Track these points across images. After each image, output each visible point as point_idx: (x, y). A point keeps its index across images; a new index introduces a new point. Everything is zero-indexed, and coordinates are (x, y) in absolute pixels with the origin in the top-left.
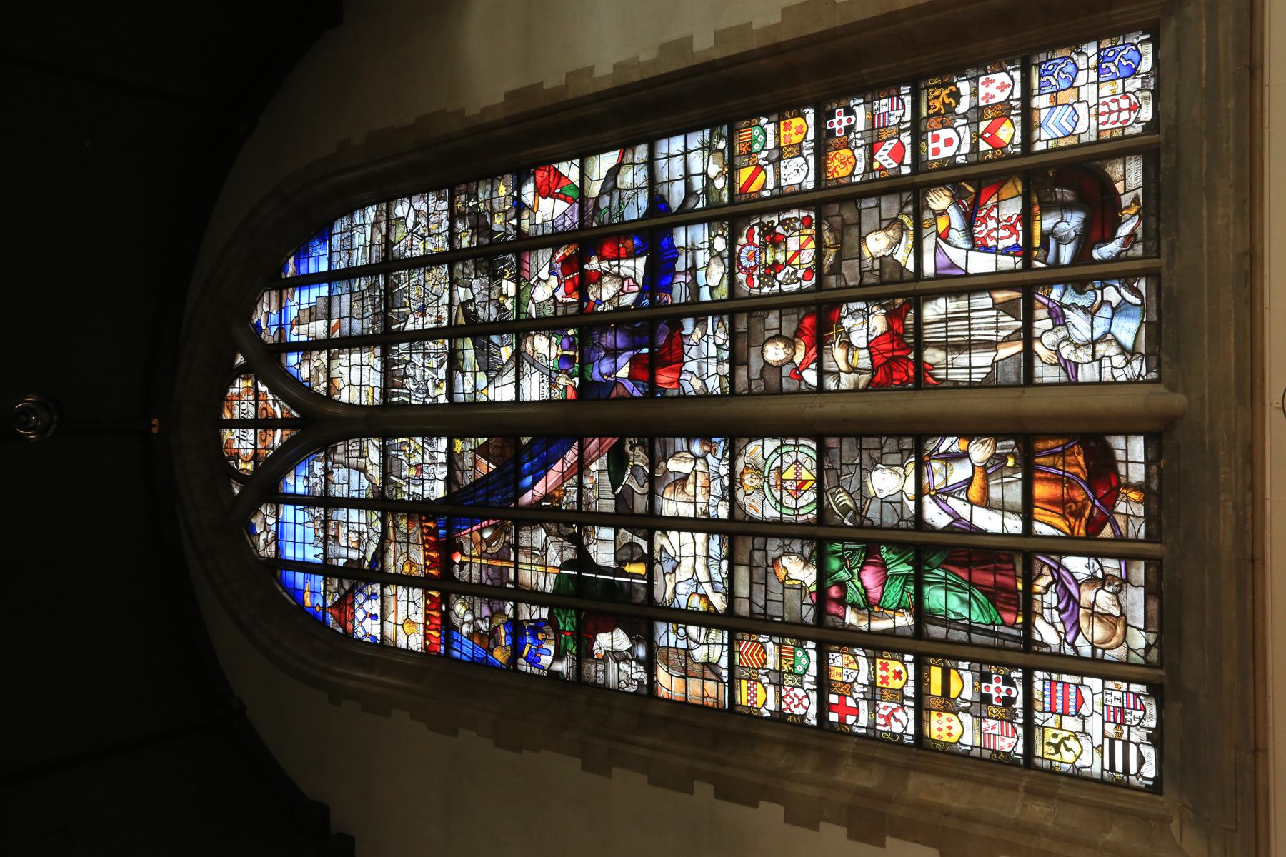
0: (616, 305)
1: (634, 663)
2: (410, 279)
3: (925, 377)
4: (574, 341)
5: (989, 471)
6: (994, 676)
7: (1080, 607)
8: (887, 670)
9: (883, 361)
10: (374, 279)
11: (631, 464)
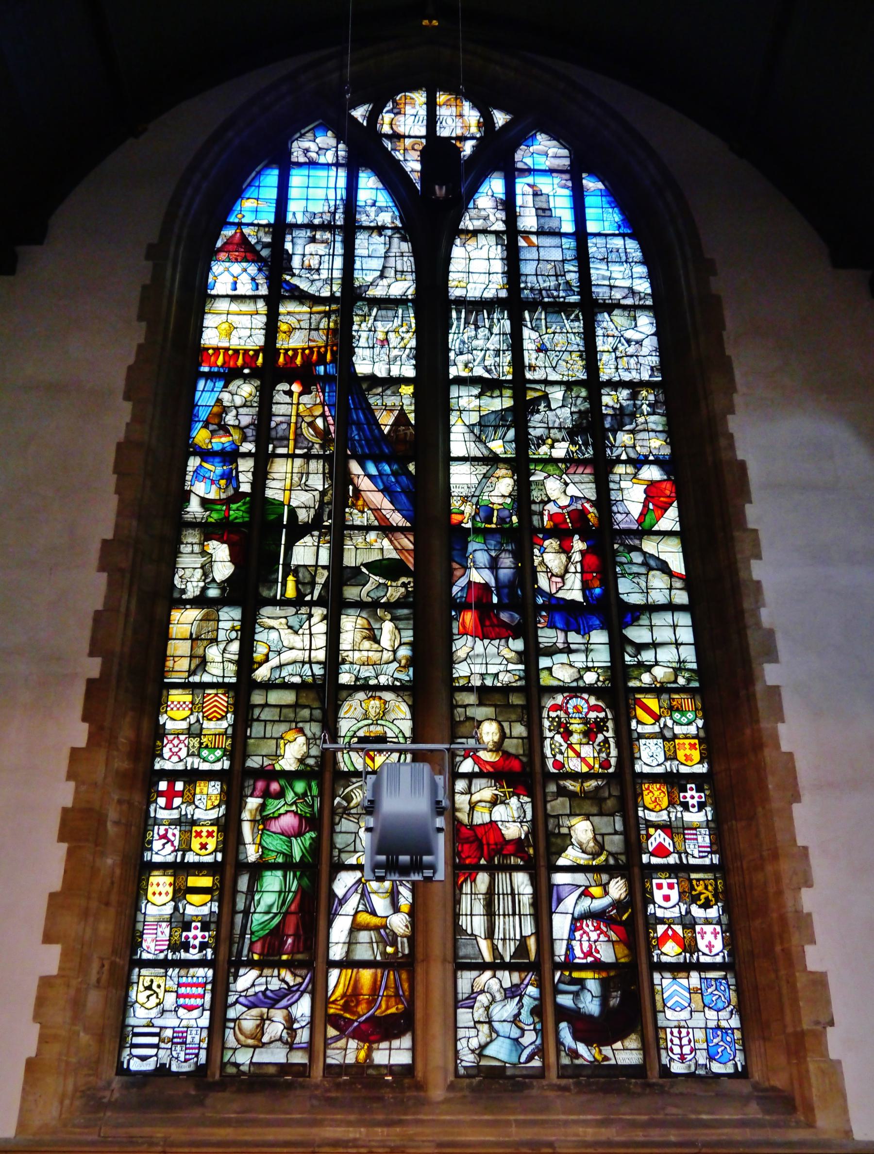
0: (539, 569)
1: (202, 584)
2: (574, 333)
3: (464, 874)
4: (507, 523)
5: (382, 931)
6: (207, 934)
7: (269, 1009)
8: (207, 837)
9: (480, 836)
10: (576, 289)
11: (389, 583)
